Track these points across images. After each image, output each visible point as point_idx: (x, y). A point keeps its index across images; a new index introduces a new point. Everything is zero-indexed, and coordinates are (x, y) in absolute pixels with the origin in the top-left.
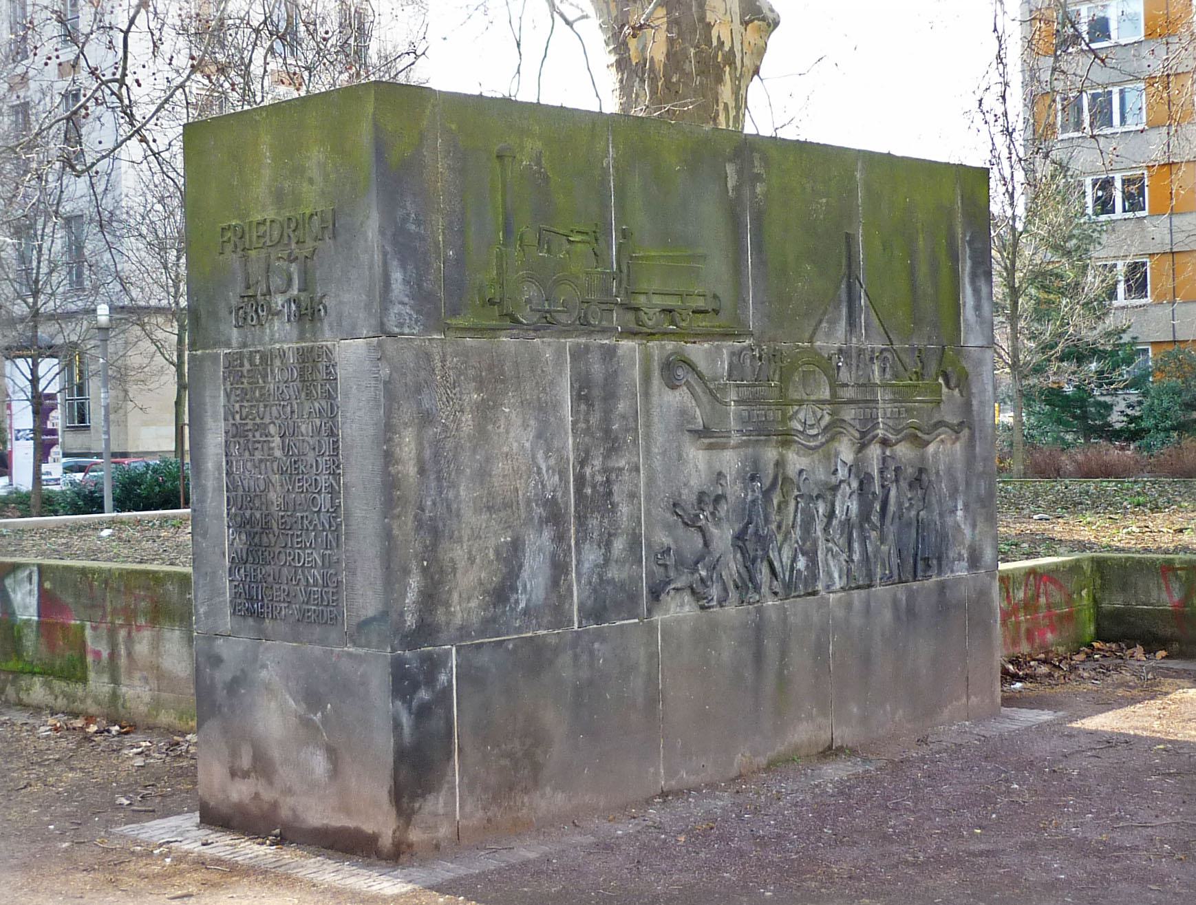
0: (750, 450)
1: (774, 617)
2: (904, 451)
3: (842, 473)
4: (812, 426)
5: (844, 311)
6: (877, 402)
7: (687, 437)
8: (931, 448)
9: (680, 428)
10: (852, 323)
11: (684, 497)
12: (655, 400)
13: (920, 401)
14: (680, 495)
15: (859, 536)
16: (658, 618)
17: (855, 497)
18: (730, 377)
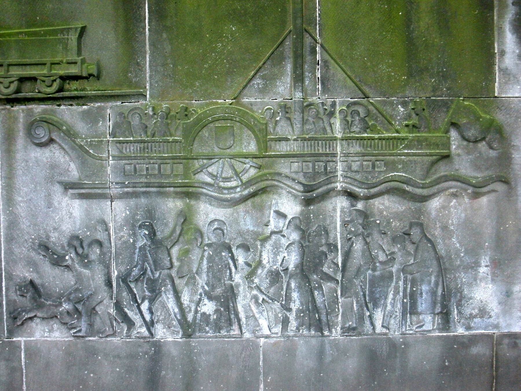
0: (143, 200)
1: (174, 352)
2: (386, 205)
3: (274, 223)
4: (227, 179)
5: (289, 67)
6: (334, 155)
7: (58, 189)
8: (435, 204)
9: (50, 180)
10: (298, 78)
11: (53, 239)
12: (19, 156)
13: (408, 155)
14: (48, 237)
15: (300, 287)
16: (21, 339)
17: (295, 248)
18: (113, 134)
